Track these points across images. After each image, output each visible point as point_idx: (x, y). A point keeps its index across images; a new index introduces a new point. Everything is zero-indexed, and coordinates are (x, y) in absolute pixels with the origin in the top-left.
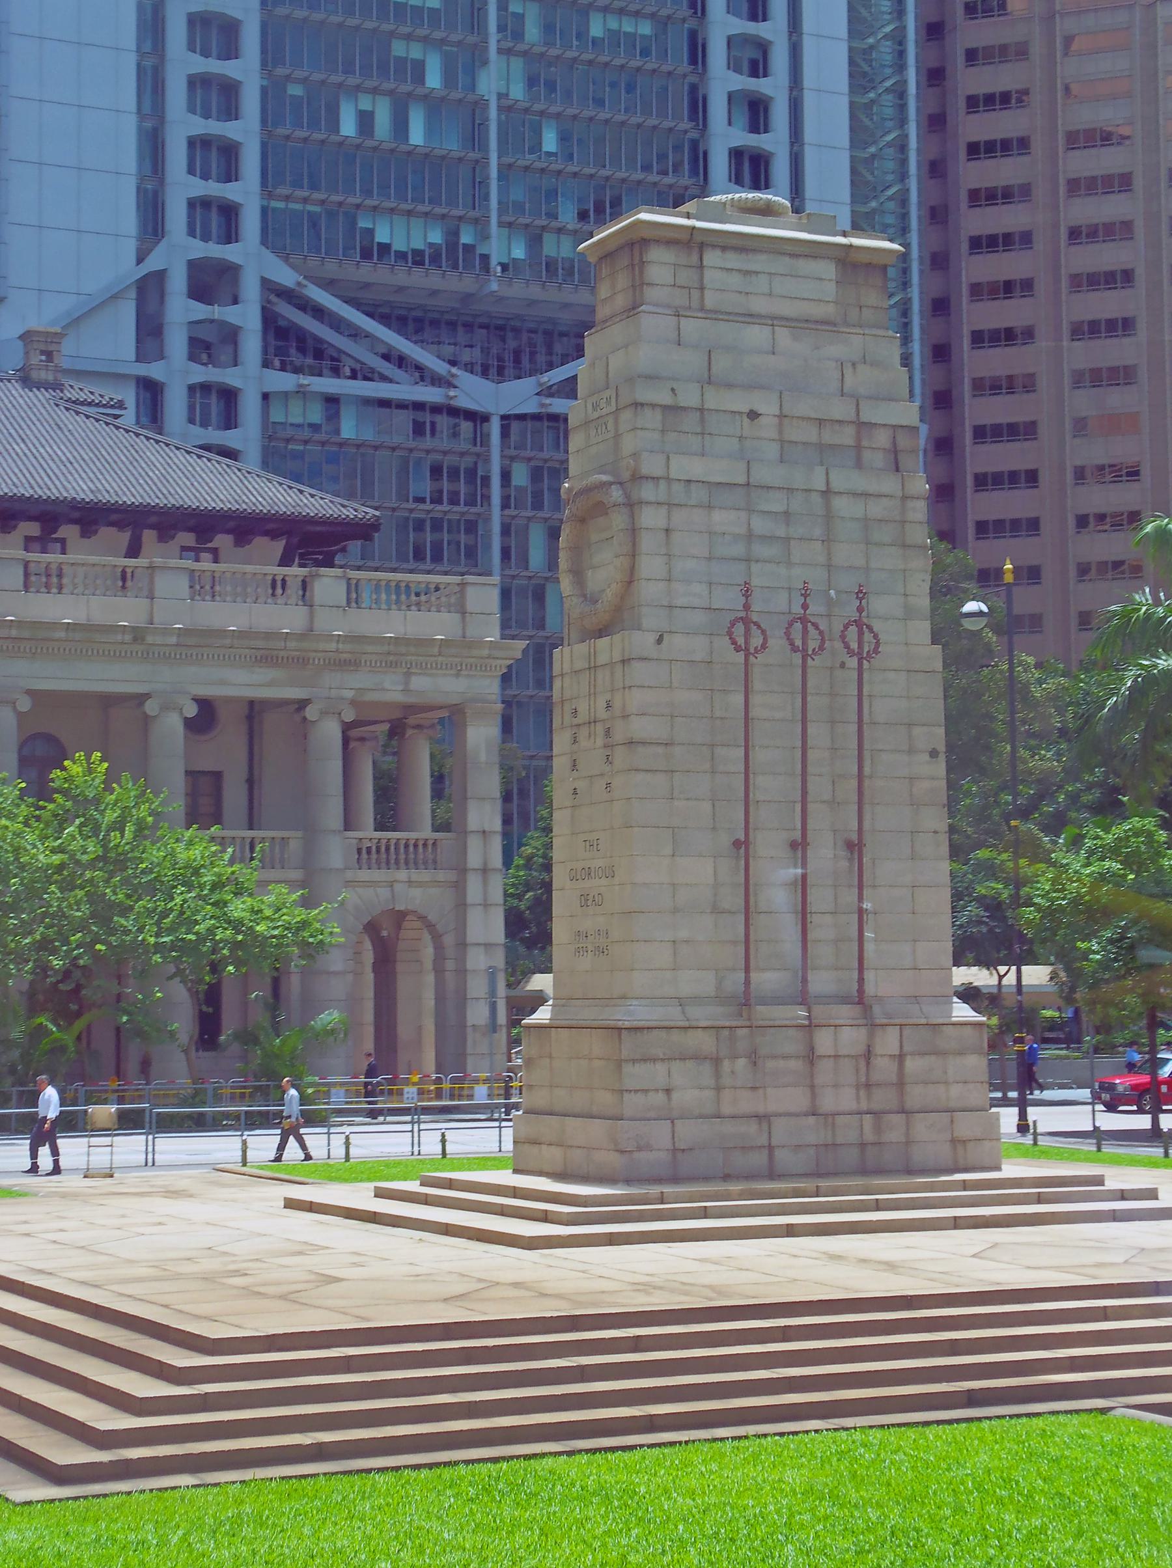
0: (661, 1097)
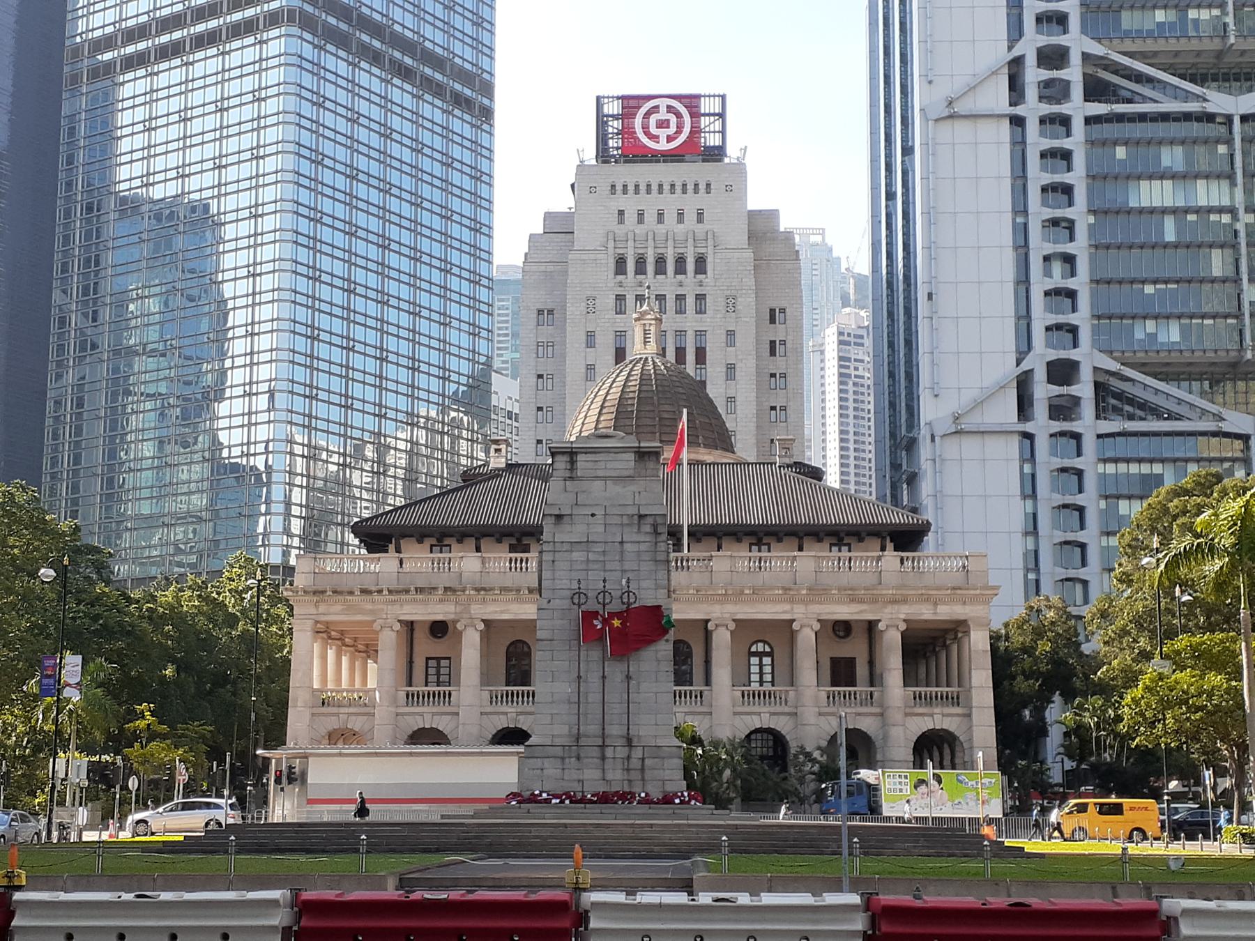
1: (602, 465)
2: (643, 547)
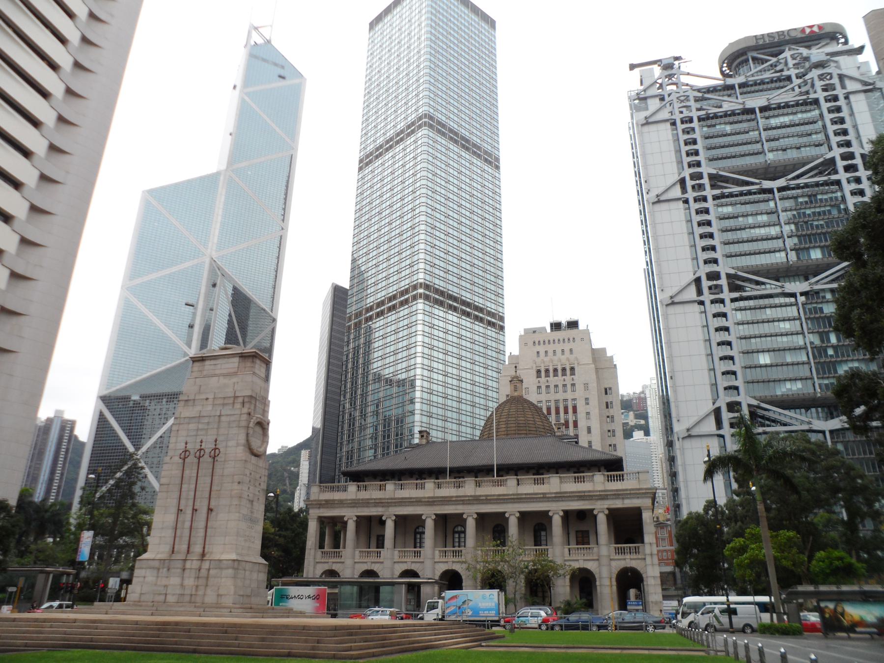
1: (219, 366)
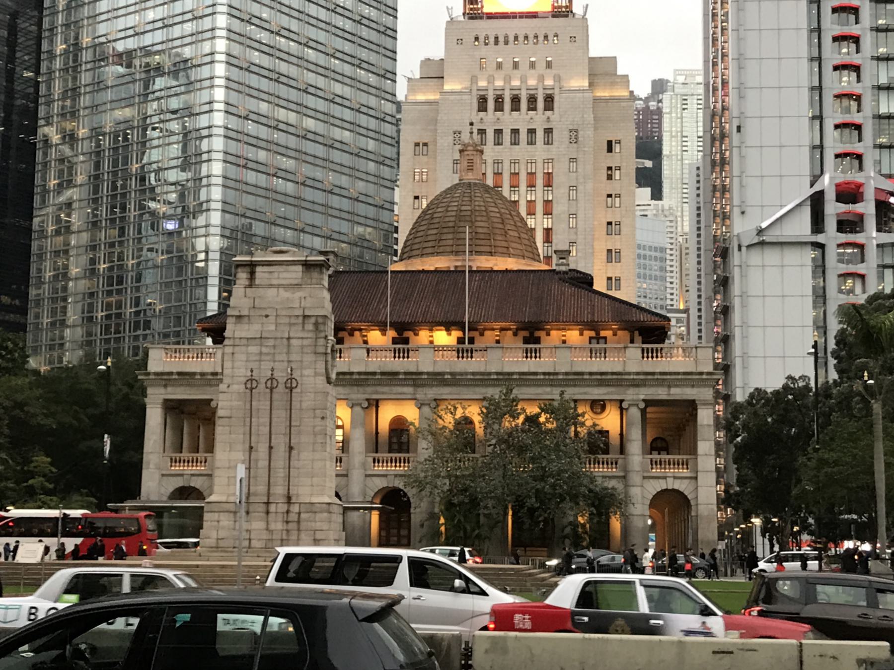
0: (216, 523)
1: (276, 275)
2: (306, 342)
